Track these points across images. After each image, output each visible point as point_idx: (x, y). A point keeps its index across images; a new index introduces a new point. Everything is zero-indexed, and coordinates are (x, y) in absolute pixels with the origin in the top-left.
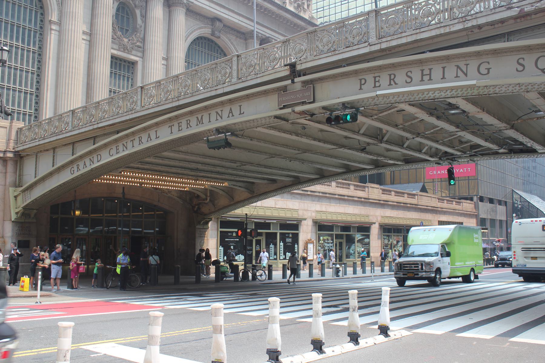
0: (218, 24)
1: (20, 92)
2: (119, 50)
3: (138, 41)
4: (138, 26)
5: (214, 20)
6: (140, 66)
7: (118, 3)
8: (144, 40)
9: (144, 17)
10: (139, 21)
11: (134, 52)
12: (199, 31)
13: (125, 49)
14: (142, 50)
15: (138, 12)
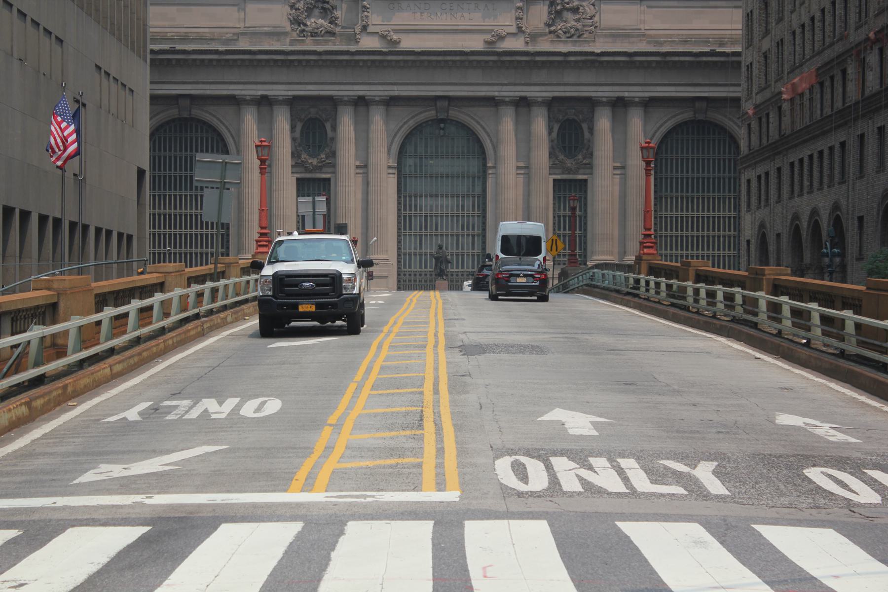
0: (697, 104)
1: (468, 236)
2: (563, 173)
3: (584, 158)
4: (585, 142)
5: (693, 100)
6: (589, 185)
7: (559, 125)
8: (592, 154)
9: (591, 130)
10: (587, 134)
11: (581, 171)
12: (673, 120)
13: (569, 171)
14: (590, 166)
15: (585, 126)
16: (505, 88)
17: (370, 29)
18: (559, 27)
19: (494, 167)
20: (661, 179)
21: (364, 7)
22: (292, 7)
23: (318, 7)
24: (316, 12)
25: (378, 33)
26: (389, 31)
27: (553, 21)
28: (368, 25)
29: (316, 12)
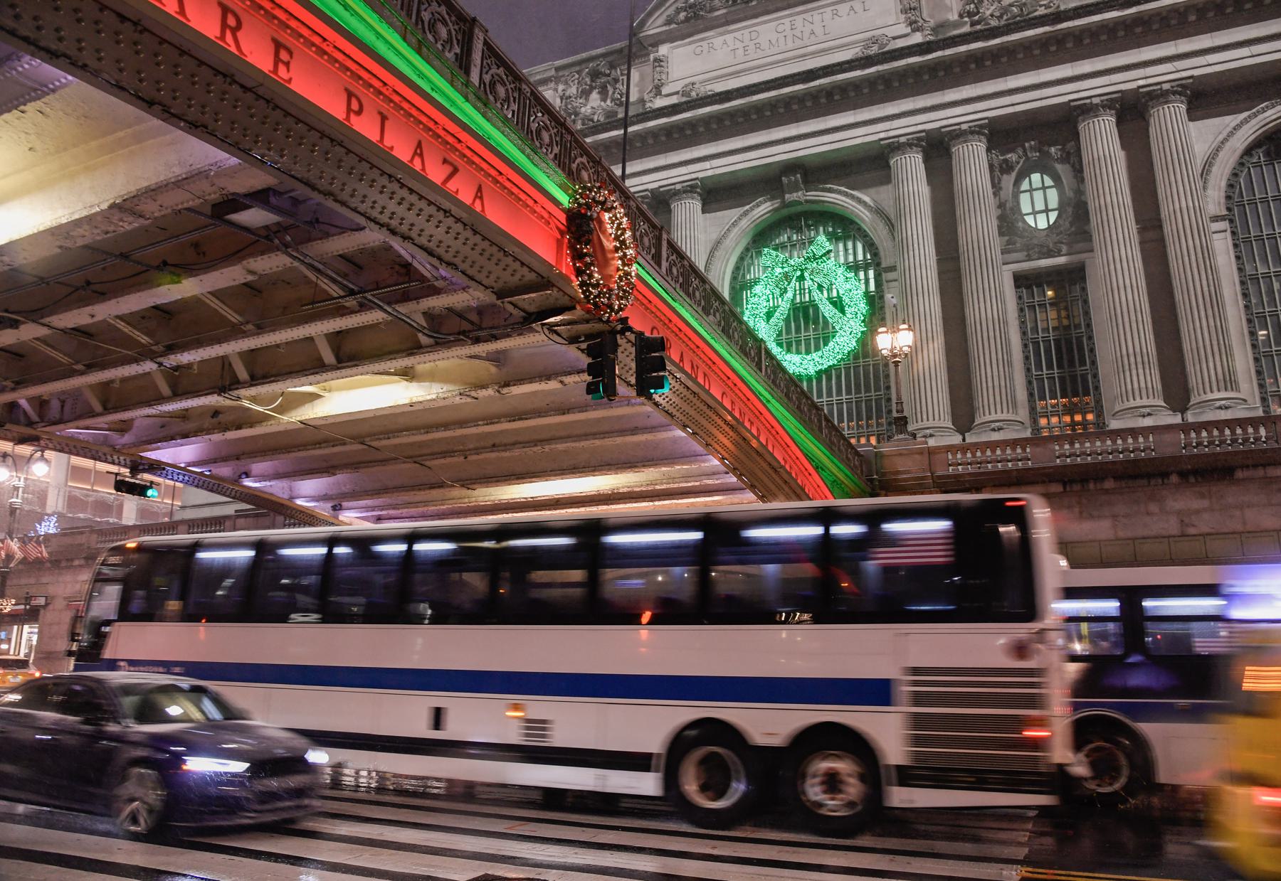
2: (1029, 258)
6: (1089, 272)
16: (897, 123)
17: (665, 91)
18: (988, 13)
19: (892, 269)
20: (1248, 242)
21: (656, 60)
22: (562, 99)
23: (595, 88)
24: (595, 95)
25: (677, 93)
26: (693, 84)
27: (976, 7)
28: (663, 84)
29: (595, 95)
